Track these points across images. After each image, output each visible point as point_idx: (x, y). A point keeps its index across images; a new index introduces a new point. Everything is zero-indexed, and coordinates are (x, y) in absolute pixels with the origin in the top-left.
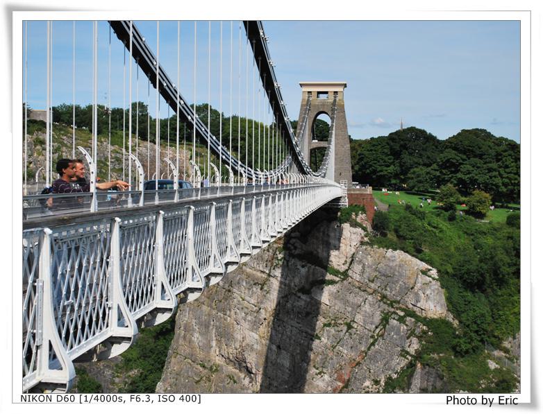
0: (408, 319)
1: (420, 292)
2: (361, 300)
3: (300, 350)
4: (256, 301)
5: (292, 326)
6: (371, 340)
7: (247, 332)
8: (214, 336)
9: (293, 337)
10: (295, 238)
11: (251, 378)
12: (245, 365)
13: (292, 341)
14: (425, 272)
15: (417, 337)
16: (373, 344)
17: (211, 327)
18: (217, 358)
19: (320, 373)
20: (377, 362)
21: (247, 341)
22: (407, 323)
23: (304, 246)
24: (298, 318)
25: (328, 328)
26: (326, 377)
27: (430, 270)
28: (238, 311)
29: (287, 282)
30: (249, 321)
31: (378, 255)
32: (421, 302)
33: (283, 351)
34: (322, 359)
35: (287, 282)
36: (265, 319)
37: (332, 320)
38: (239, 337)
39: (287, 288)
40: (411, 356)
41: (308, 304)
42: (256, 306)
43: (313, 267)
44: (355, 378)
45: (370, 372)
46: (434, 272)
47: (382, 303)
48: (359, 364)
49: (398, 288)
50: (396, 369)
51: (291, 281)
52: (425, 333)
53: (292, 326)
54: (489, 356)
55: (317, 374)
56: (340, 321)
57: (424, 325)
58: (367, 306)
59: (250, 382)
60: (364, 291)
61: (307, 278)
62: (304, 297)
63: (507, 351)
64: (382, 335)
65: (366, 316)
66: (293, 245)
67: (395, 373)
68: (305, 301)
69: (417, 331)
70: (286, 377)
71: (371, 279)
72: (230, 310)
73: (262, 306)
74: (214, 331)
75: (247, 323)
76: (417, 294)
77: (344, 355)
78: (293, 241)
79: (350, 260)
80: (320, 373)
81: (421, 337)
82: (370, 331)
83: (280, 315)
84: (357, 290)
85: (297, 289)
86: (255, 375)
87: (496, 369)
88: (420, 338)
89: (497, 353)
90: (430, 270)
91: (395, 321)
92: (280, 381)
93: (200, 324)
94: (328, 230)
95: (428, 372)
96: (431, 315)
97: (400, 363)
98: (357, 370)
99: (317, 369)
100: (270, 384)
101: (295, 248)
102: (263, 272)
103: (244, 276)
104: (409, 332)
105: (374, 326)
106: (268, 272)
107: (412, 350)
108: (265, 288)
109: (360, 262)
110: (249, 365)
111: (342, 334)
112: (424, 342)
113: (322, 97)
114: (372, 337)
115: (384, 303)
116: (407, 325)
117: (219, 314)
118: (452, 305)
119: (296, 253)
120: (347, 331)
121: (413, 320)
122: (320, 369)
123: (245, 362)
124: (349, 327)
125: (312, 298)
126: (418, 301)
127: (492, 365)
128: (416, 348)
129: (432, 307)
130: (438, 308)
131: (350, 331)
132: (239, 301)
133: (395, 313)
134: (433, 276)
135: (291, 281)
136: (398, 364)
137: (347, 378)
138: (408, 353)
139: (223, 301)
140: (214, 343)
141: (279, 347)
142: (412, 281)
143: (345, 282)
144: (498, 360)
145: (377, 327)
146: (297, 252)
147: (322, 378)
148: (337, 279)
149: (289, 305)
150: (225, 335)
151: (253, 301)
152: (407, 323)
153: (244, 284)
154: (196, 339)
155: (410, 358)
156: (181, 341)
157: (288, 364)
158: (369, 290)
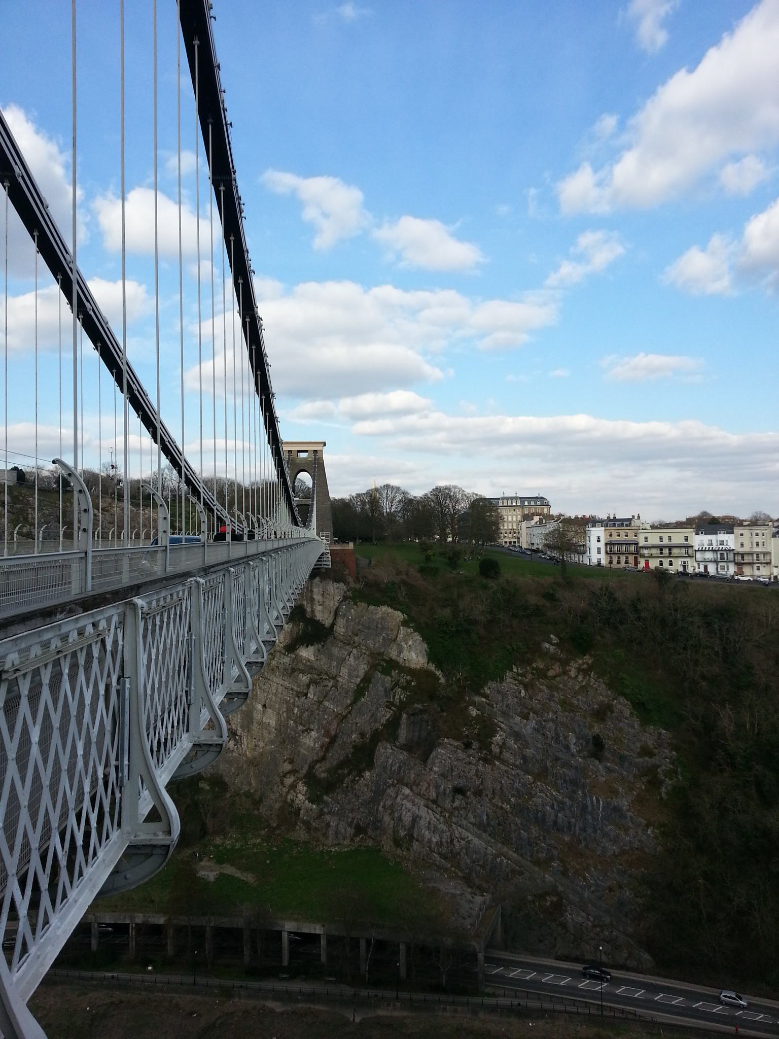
5: (277, 684)
11: (236, 740)
19: (306, 730)
20: (364, 715)
26: (313, 734)
31: (360, 608)
33: (269, 710)
34: (308, 715)
49: (381, 640)
50: (382, 721)
52: (409, 682)
53: (277, 684)
54: (473, 703)
59: (235, 745)
63: (486, 696)
70: (272, 736)
80: (306, 730)
83: (266, 674)
86: (240, 737)
87: (477, 715)
88: (403, 688)
89: (477, 699)
94: (311, 586)
95: (413, 722)
96: (413, 666)
97: (385, 715)
100: (256, 746)
104: (394, 683)
109: (344, 616)
113: (302, 455)
116: (391, 677)
118: (432, 656)
122: (307, 726)
125: (297, 655)
126: (400, 652)
127: (474, 712)
129: (414, 656)
130: (420, 659)
133: (379, 664)
137: (333, 733)
138: (392, 704)
141: (264, 706)
142: (395, 633)
144: (479, 706)
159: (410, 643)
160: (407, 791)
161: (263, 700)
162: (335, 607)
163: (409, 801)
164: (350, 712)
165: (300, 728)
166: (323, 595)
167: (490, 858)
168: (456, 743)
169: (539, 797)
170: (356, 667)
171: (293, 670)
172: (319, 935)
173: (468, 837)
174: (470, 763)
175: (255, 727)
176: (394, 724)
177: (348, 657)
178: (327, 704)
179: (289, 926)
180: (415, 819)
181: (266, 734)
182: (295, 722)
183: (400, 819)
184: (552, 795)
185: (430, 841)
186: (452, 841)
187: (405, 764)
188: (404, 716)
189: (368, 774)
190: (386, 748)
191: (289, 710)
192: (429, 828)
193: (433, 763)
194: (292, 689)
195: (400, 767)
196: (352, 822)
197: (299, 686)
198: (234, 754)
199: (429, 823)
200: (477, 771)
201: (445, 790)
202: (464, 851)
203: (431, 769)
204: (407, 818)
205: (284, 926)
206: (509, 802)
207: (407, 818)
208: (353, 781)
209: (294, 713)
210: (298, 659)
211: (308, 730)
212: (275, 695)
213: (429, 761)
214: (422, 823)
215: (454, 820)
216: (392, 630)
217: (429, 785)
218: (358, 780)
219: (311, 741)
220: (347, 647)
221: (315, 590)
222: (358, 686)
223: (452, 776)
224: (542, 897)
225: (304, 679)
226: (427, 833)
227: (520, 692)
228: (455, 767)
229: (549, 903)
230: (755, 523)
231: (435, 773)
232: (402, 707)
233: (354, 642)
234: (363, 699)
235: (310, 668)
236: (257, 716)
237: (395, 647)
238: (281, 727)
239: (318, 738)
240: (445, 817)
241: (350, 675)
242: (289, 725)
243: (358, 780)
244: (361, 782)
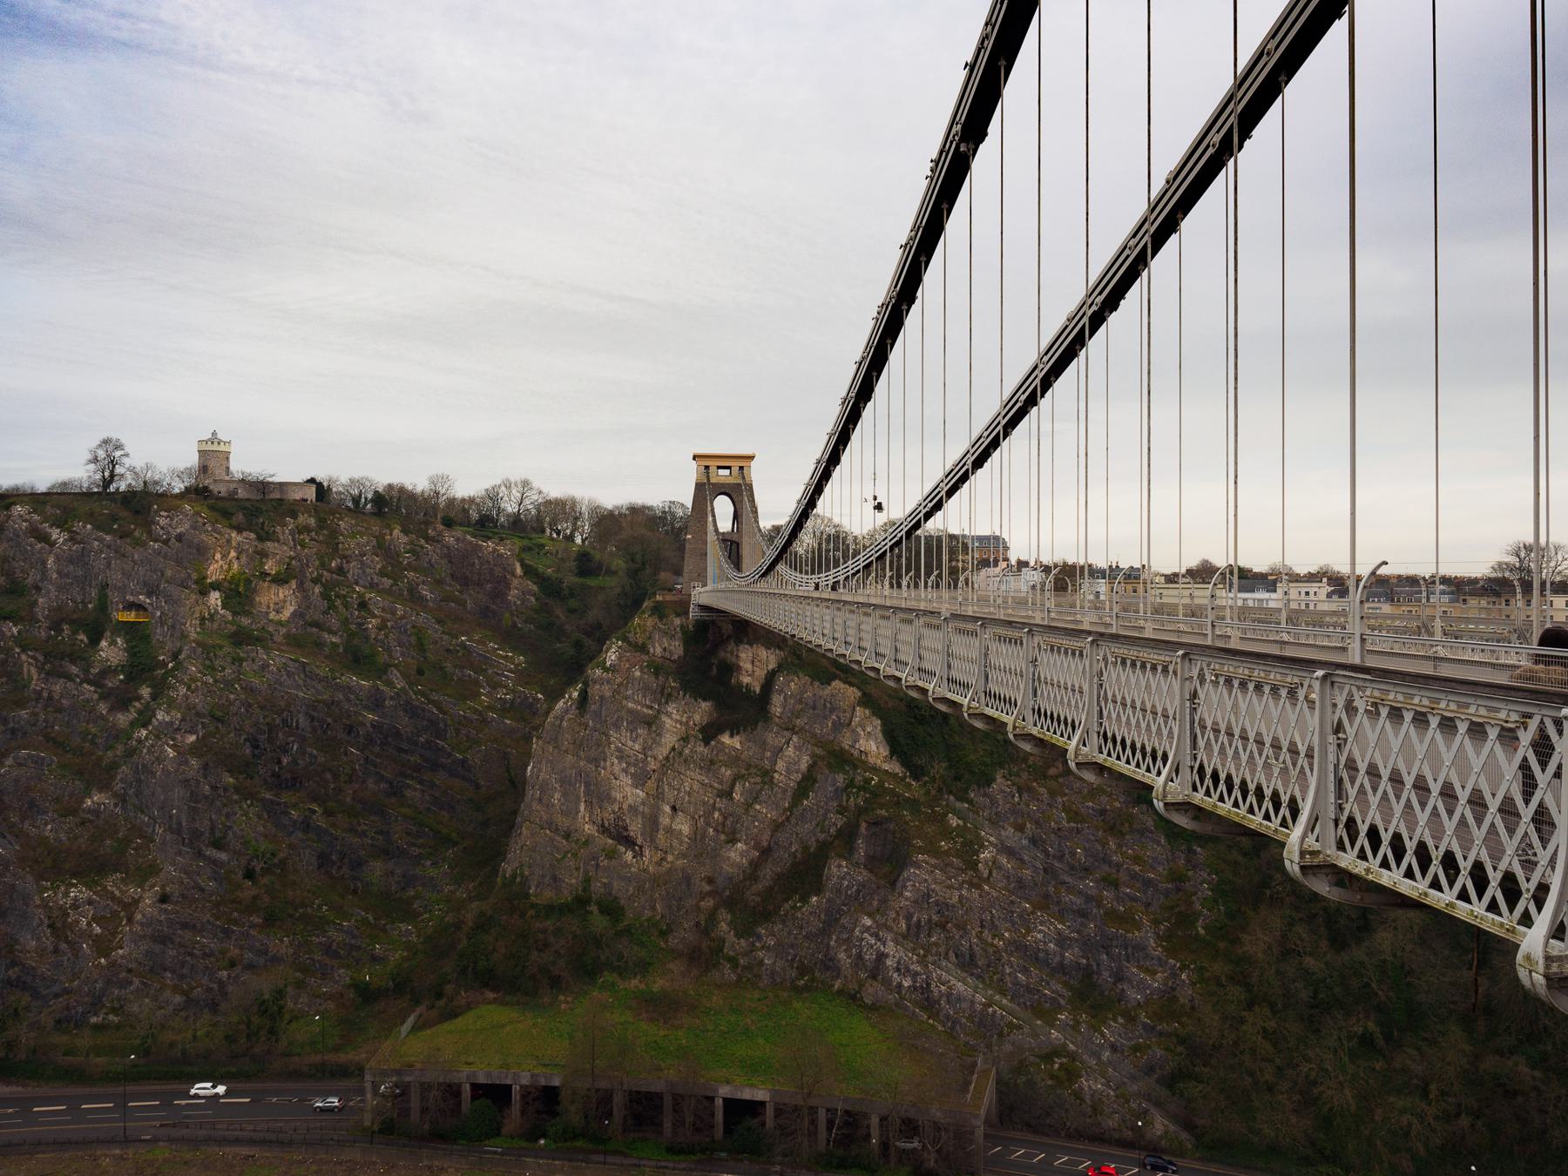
1: (859, 729)
2: (784, 741)
7: (628, 789)
11: (634, 851)
12: (625, 834)
18: (587, 826)
24: (701, 768)
28: (616, 761)
30: (631, 774)
32: (861, 742)
34: (733, 822)
35: (684, 720)
36: (654, 771)
38: (619, 796)
49: (830, 725)
51: (689, 718)
59: (634, 857)
72: (605, 761)
76: (854, 731)
86: (641, 847)
92: (676, 853)
93: (562, 781)
102: (651, 708)
103: (623, 713)
108: (654, 729)
109: (781, 691)
110: (632, 834)
123: (627, 830)
127: (954, 821)
129: (874, 747)
130: (881, 750)
132: (617, 747)
137: (765, 844)
140: (582, 808)
141: (674, 808)
142: (848, 715)
150: (599, 795)
151: (637, 747)
156: (535, 806)
159: (869, 729)
160: (868, 922)
161: (672, 800)
163: (871, 935)
164: (788, 819)
165: (723, 837)
166: (753, 662)
167: (979, 1007)
168: (933, 861)
169: (1040, 931)
170: (796, 759)
172: (763, 1104)
173: (949, 982)
174: (950, 887)
175: (661, 835)
176: (847, 837)
178: (758, 807)
179: (724, 1091)
180: (881, 957)
181: (675, 843)
182: (715, 830)
183: (859, 956)
184: (1056, 928)
185: (900, 985)
186: (928, 985)
187: (864, 886)
188: (864, 825)
189: (815, 899)
190: (839, 866)
191: (708, 814)
192: (898, 970)
193: (904, 887)
194: (711, 786)
195: (858, 891)
196: (793, 960)
197: (721, 783)
198: (633, 869)
199: (899, 962)
200: (961, 896)
201: (919, 921)
202: (944, 999)
203: (901, 894)
204: (869, 956)
205: (716, 1091)
206: (1002, 937)
207: (869, 956)
208: (794, 907)
211: (732, 840)
212: (689, 794)
213: (899, 884)
214: (889, 962)
215: (930, 958)
216: (845, 711)
217: (898, 915)
218: (801, 907)
219: (738, 854)
221: (743, 655)
222: (799, 783)
223: (928, 903)
224: (1048, 1057)
225: (727, 773)
226: (895, 975)
227: (1014, 796)
228: (933, 891)
229: (1057, 1066)
230: (1312, 578)
231: (907, 899)
232: (860, 811)
233: (794, 726)
234: (805, 802)
235: (735, 760)
236: (665, 821)
238: (697, 836)
239: (747, 851)
240: (918, 955)
241: (788, 771)
243: (801, 907)
244: (804, 909)
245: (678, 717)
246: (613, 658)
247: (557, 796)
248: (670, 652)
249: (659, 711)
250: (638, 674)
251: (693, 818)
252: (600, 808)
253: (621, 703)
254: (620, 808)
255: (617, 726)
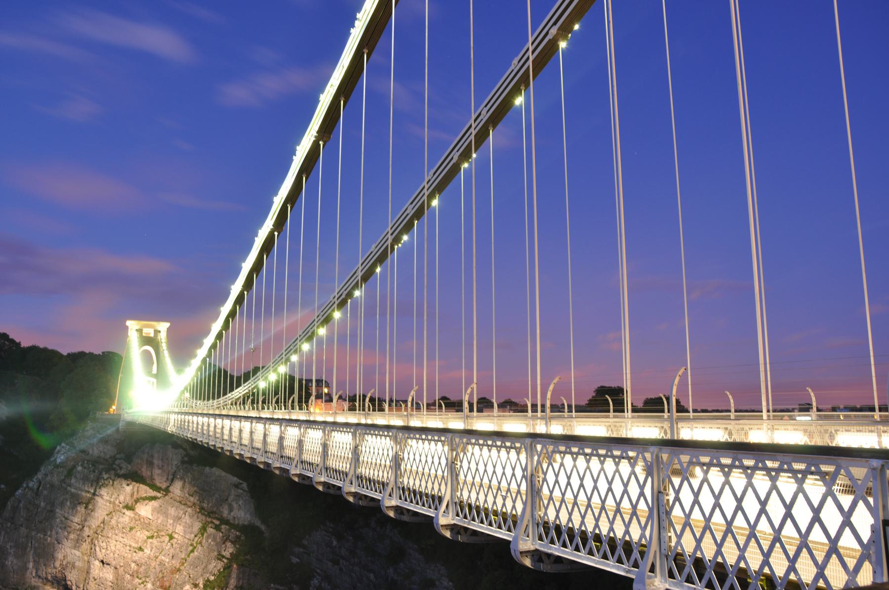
0: (223, 527)
2: (182, 512)
3: (124, 563)
4: (79, 520)
5: (116, 541)
6: (191, 548)
8: (31, 557)
9: (117, 551)
10: (119, 459)
13: (116, 555)
14: (237, 486)
15: (232, 542)
16: (192, 551)
17: (29, 549)
18: (33, 580)
19: (143, 583)
21: (69, 559)
22: (222, 530)
23: (129, 466)
25: (151, 540)
27: (241, 484)
28: (60, 530)
29: (112, 500)
34: (145, 570)
36: (88, 536)
37: (155, 532)
39: (111, 505)
40: (227, 559)
41: (131, 519)
42: (79, 524)
43: (138, 485)
44: (176, 583)
45: (190, 577)
46: (245, 485)
47: (200, 514)
48: (179, 570)
49: (214, 501)
50: (213, 572)
51: (116, 498)
55: (140, 584)
56: (162, 533)
57: (237, 531)
58: (187, 517)
60: (184, 505)
61: (132, 495)
62: (129, 513)
64: (201, 543)
65: (186, 527)
66: (118, 466)
67: (213, 576)
68: (130, 517)
69: (232, 537)
71: (191, 493)
73: (87, 524)
74: (32, 552)
75: (69, 541)
77: (166, 564)
78: (117, 462)
79: (172, 477)
80: (143, 583)
81: (235, 541)
82: (190, 540)
84: (179, 503)
85: (121, 505)
89: (297, 550)
90: (241, 484)
91: (212, 530)
98: (177, 577)
99: (140, 579)
101: (121, 468)
104: (225, 538)
105: (193, 536)
106: (92, 491)
107: (227, 554)
110: (69, 583)
111: (164, 544)
112: (238, 546)
114: (192, 545)
115: (202, 514)
116: (222, 533)
117: (39, 535)
119: (121, 473)
120: (169, 542)
121: (227, 527)
122: (144, 579)
124: (171, 537)
125: (136, 514)
126: (231, 510)
128: (231, 552)
131: (171, 541)
132: (62, 521)
134: (244, 489)
135: (116, 498)
136: (215, 567)
138: (223, 557)
139: (44, 522)
140: (31, 565)
143: (167, 497)
145: (196, 536)
146: (122, 472)
147: (145, 587)
148: (159, 495)
149: (113, 522)
152: (222, 530)
153: (68, 503)
154: (10, 563)
155: (225, 561)
157: (111, 577)
158: (188, 503)
162: (173, 471)
165: (137, 581)
171: (131, 529)
177: (184, 515)
182: (132, 575)
197: (137, 542)
209: (131, 568)
210: (138, 518)
220: (183, 507)
227: (332, 543)
235: (146, 525)
237: (226, 507)
242: (126, 579)
245: (108, 498)
246: (62, 458)
247: (10, 558)
248: (104, 453)
249: (94, 494)
250: (79, 468)
251: (116, 568)
252: (44, 565)
253: (66, 489)
254: (60, 564)
255: (62, 504)
